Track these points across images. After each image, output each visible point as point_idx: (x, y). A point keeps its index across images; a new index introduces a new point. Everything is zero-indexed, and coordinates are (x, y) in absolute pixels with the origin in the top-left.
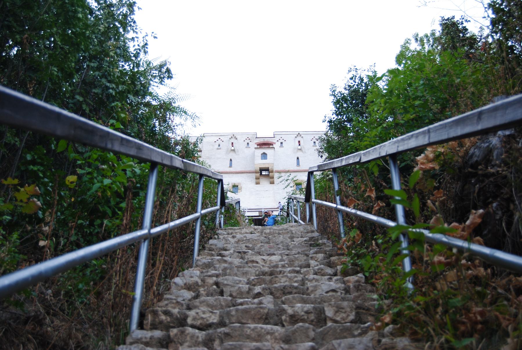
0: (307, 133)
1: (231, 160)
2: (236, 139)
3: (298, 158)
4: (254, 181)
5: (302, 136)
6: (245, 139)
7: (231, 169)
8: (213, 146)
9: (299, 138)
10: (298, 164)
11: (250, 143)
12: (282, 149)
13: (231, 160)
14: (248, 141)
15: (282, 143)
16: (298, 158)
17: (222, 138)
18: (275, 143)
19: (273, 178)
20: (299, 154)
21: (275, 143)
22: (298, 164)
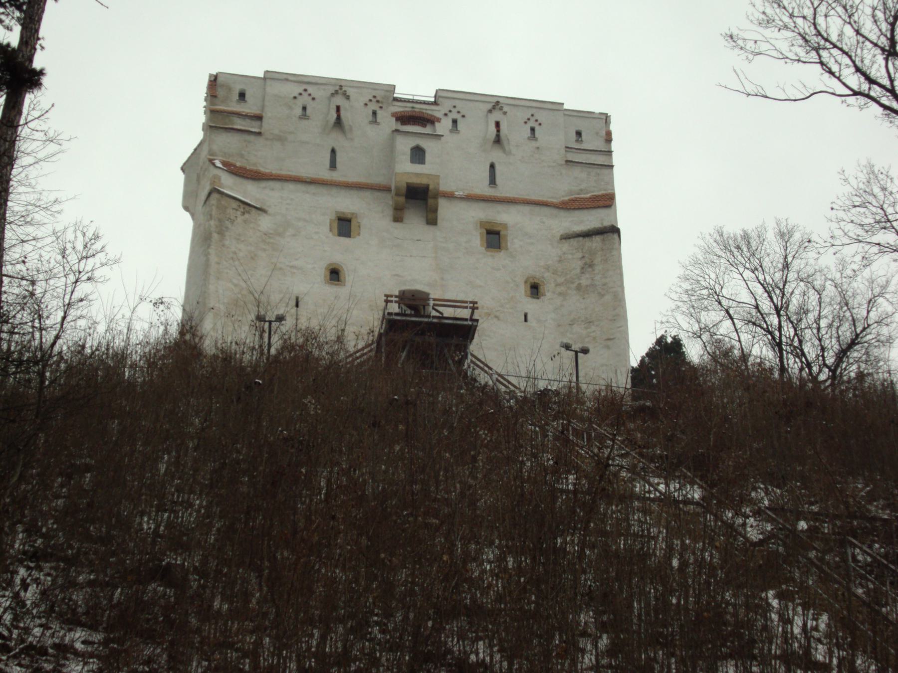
0: (516, 103)
1: (333, 151)
2: (348, 98)
3: (492, 166)
4: (390, 212)
5: (505, 109)
6: (366, 100)
7: (336, 176)
8: (290, 108)
9: (497, 116)
10: (493, 181)
11: (379, 112)
12: (455, 137)
13: (333, 151)
14: (373, 106)
15: (455, 122)
16: (492, 166)
17: (311, 89)
18: (439, 120)
19: (435, 210)
20: (496, 156)
21: (439, 120)
22: (493, 181)
